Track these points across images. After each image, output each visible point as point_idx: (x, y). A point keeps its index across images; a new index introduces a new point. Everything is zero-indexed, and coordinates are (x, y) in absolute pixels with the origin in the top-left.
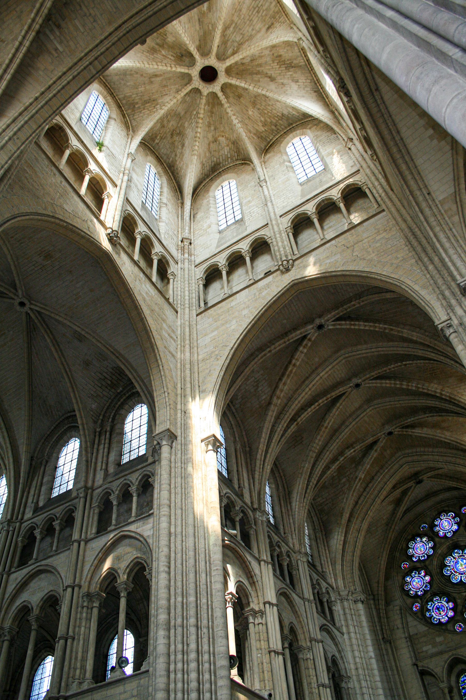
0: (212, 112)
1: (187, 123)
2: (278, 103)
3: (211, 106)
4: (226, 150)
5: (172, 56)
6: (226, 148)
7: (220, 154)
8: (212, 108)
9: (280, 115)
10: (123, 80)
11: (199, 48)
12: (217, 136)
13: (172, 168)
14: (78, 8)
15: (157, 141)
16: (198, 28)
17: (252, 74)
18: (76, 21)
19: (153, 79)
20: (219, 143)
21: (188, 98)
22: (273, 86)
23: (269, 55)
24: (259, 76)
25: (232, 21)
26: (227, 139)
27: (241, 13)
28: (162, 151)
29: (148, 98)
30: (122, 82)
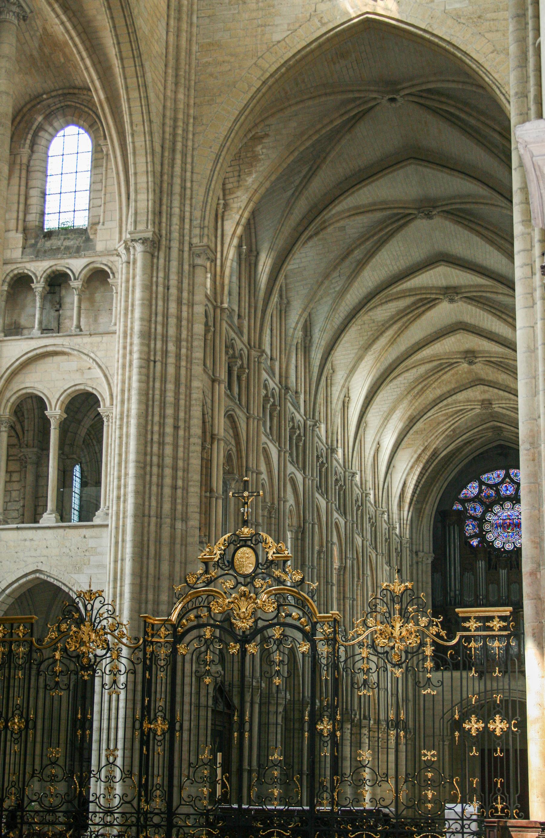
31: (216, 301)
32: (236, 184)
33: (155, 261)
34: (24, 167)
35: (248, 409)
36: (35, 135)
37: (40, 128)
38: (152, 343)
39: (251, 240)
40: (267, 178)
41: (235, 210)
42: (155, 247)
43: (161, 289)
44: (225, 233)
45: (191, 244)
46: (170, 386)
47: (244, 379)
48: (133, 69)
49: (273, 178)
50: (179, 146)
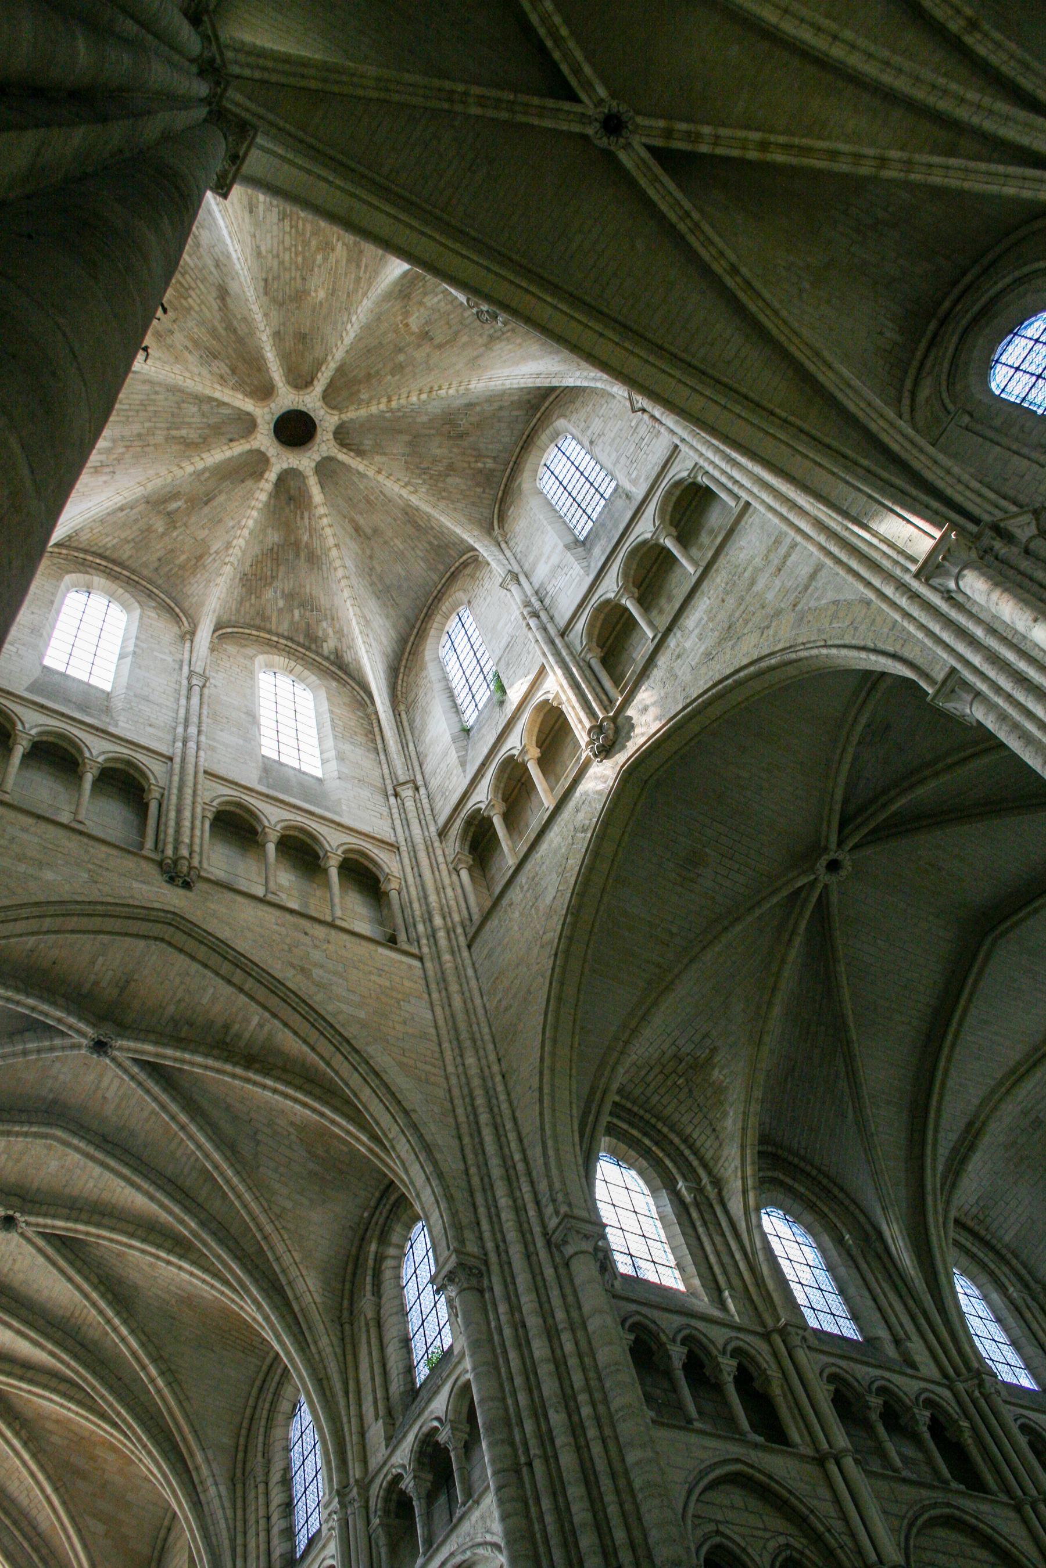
0: (369, 376)
1: (419, 420)
2: (263, 249)
3: (355, 388)
4: (431, 301)
5: (302, 518)
6: (429, 304)
7: (449, 307)
8: (360, 382)
9: (287, 223)
10: (400, 587)
11: (258, 474)
12: (413, 338)
13: (533, 402)
14: (183, 1004)
15: (490, 464)
16: (222, 498)
17: (240, 341)
18: (204, 1001)
19: (369, 531)
20: (426, 323)
21: (366, 442)
22: (233, 287)
23: (181, 330)
24: (235, 323)
25: (168, 439)
26: (407, 312)
27: (144, 431)
28: (507, 439)
29: (409, 525)
30: (405, 585)
31: (763, 1324)
32: (716, 1144)
33: (487, 1295)
34: (372, 1323)
35: (1009, 1492)
36: (377, 1273)
37: (380, 1259)
38: (516, 1431)
39: (859, 1222)
40: (748, 1102)
41: (733, 1177)
42: (480, 1274)
43: (507, 1332)
44: (735, 1218)
45: (545, 1234)
46: (575, 1491)
47: (970, 1441)
48: (346, 1063)
49: (758, 1094)
50: (484, 1118)
